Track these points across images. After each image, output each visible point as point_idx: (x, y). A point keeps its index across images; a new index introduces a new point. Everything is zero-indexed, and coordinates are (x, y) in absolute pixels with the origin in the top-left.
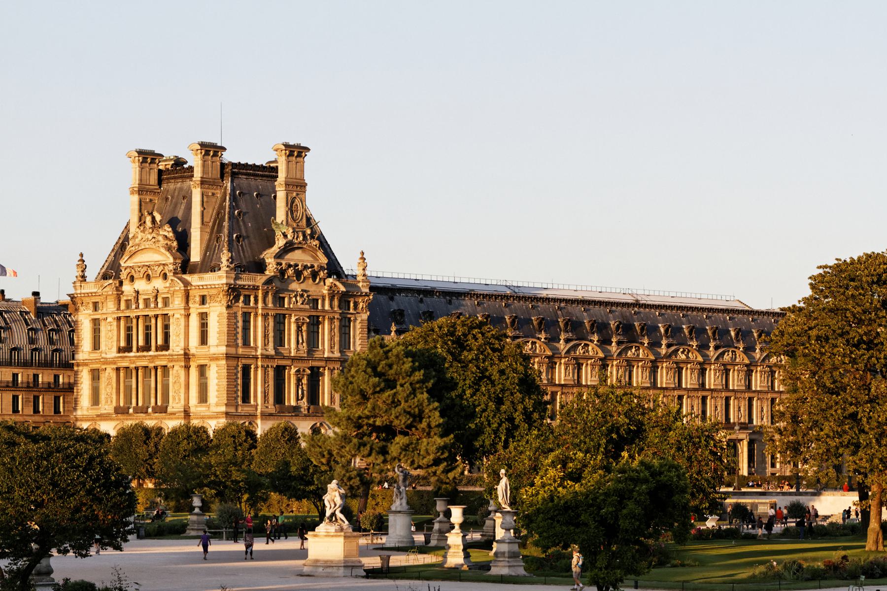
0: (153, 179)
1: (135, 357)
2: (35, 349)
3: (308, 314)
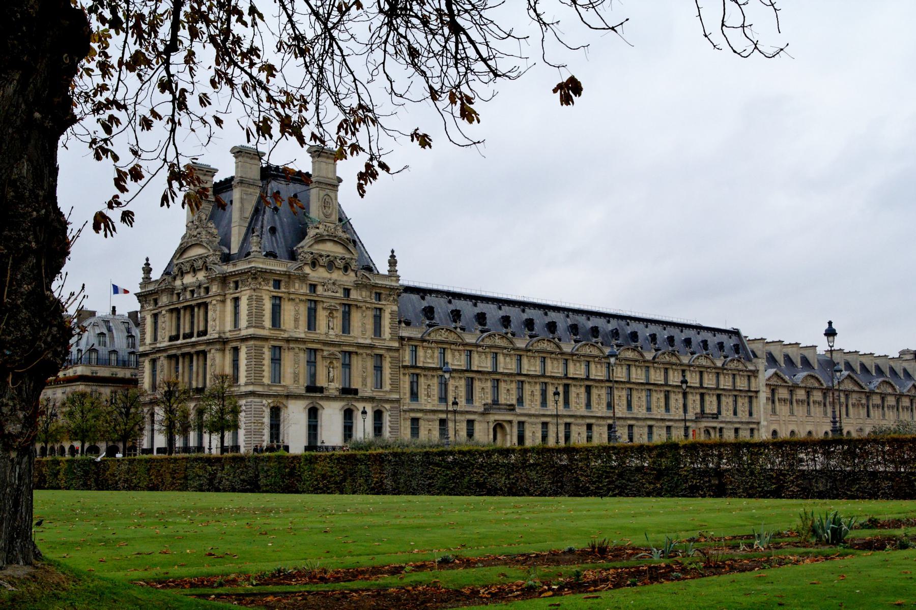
2: (133, 353)
3: (338, 302)
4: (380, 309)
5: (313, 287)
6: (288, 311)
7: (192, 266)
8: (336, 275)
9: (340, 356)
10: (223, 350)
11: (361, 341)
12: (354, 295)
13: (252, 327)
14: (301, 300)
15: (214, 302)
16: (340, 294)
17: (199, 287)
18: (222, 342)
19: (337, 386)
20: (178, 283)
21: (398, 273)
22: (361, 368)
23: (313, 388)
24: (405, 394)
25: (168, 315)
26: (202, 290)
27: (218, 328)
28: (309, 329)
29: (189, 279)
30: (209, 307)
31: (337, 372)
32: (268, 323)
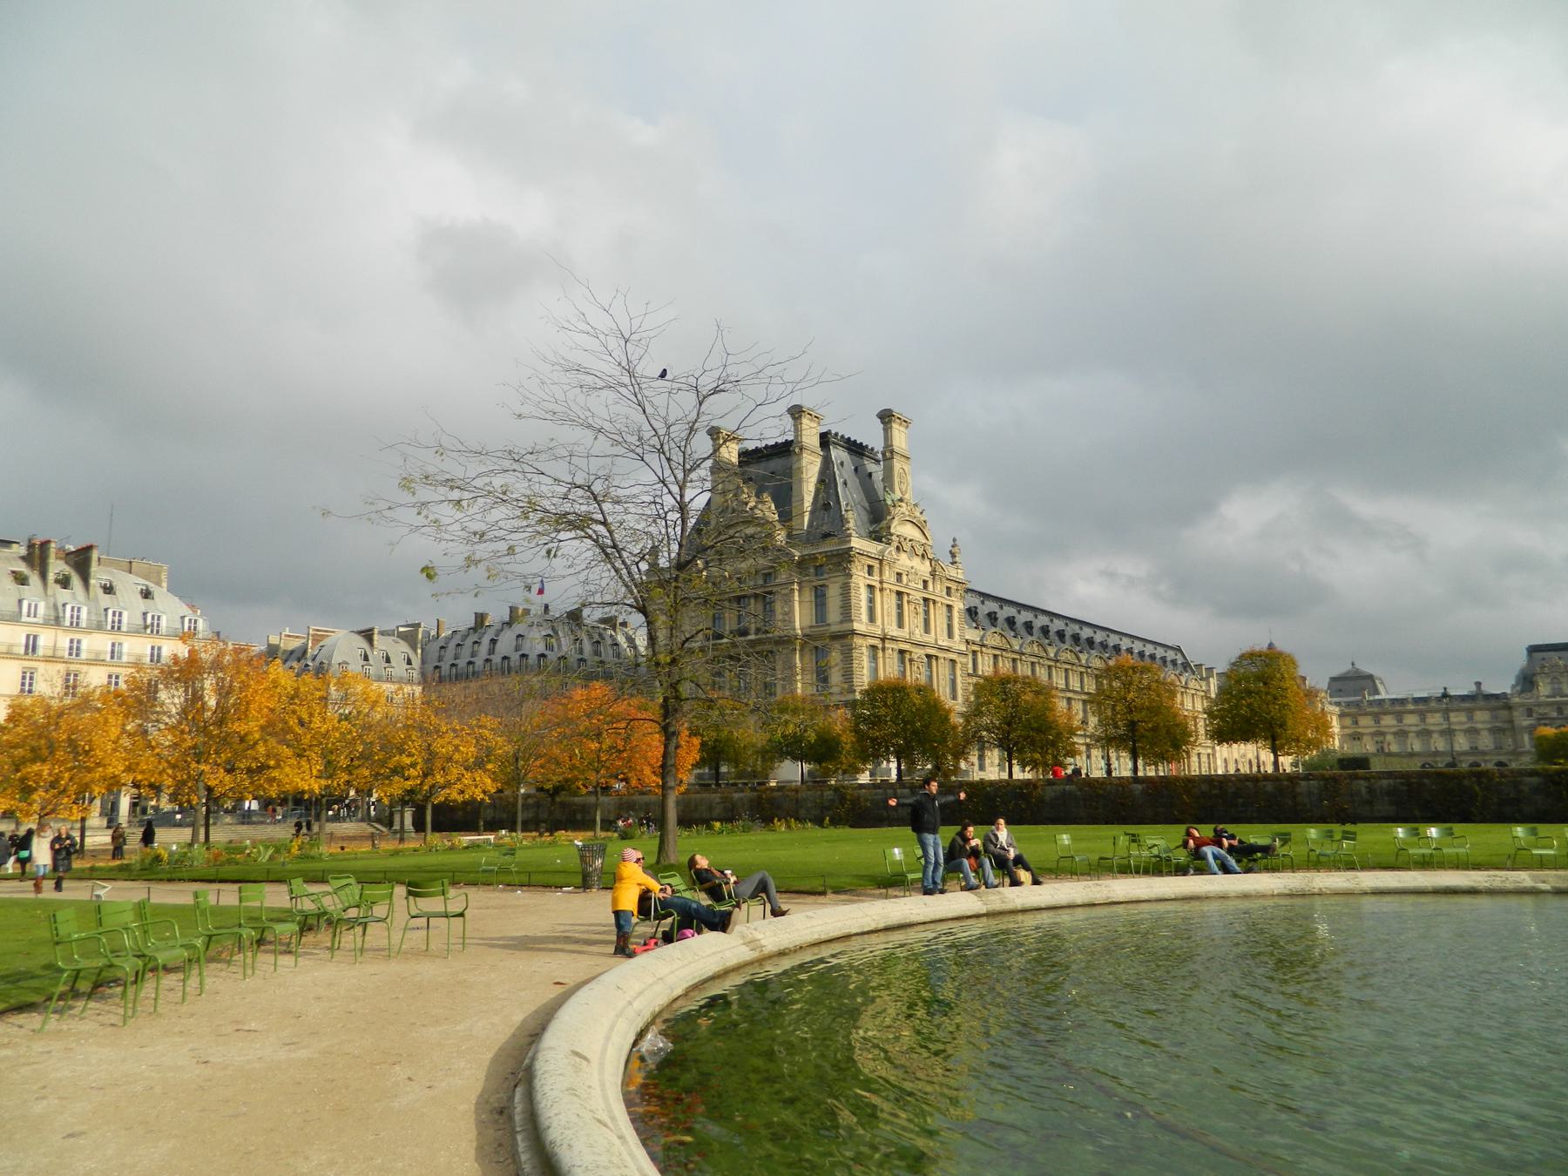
0: (735, 460)
8: (916, 562)
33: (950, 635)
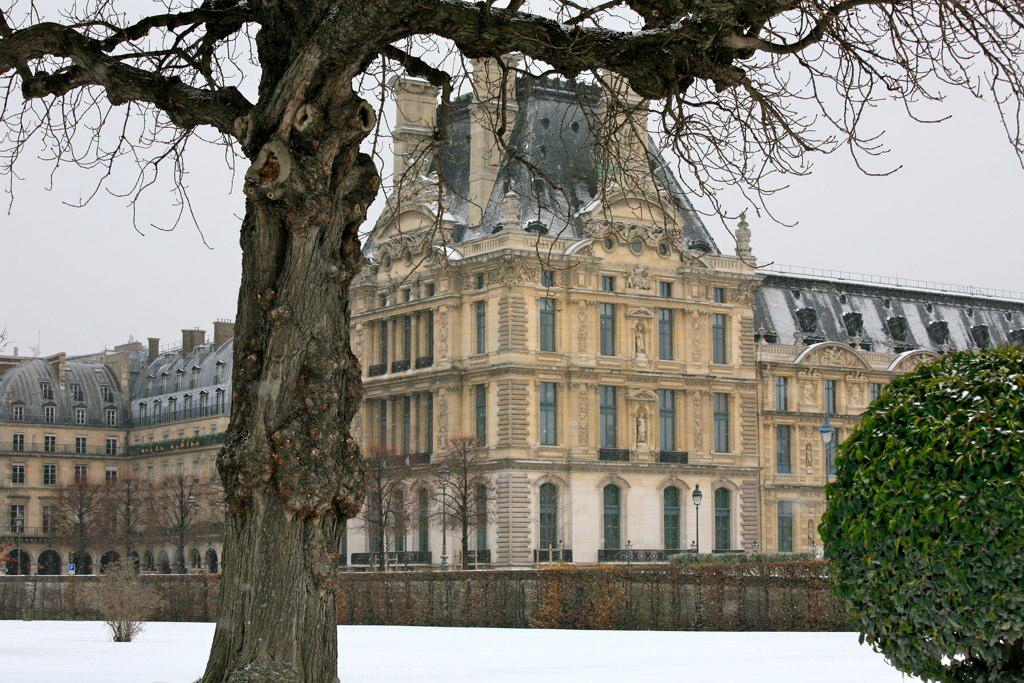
1: (390, 380)
4: (724, 316)
5: (609, 282)
6: (568, 323)
7: (406, 248)
8: (648, 259)
9: (656, 397)
10: (459, 390)
11: (690, 371)
12: (677, 290)
13: (508, 350)
14: (588, 304)
15: (443, 309)
16: (655, 290)
17: (418, 283)
18: (458, 376)
19: (652, 448)
20: (382, 277)
21: (753, 253)
22: (695, 416)
23: (611, 453)
24: (767, 460)
25: (366, 332)
26: (423, 289)
27: (449, 354)
28: (604, 352)
29: (400, 270)
30: (435, 318)
31: (652, 426)
32: (533, 343)
33: (721, 355)
